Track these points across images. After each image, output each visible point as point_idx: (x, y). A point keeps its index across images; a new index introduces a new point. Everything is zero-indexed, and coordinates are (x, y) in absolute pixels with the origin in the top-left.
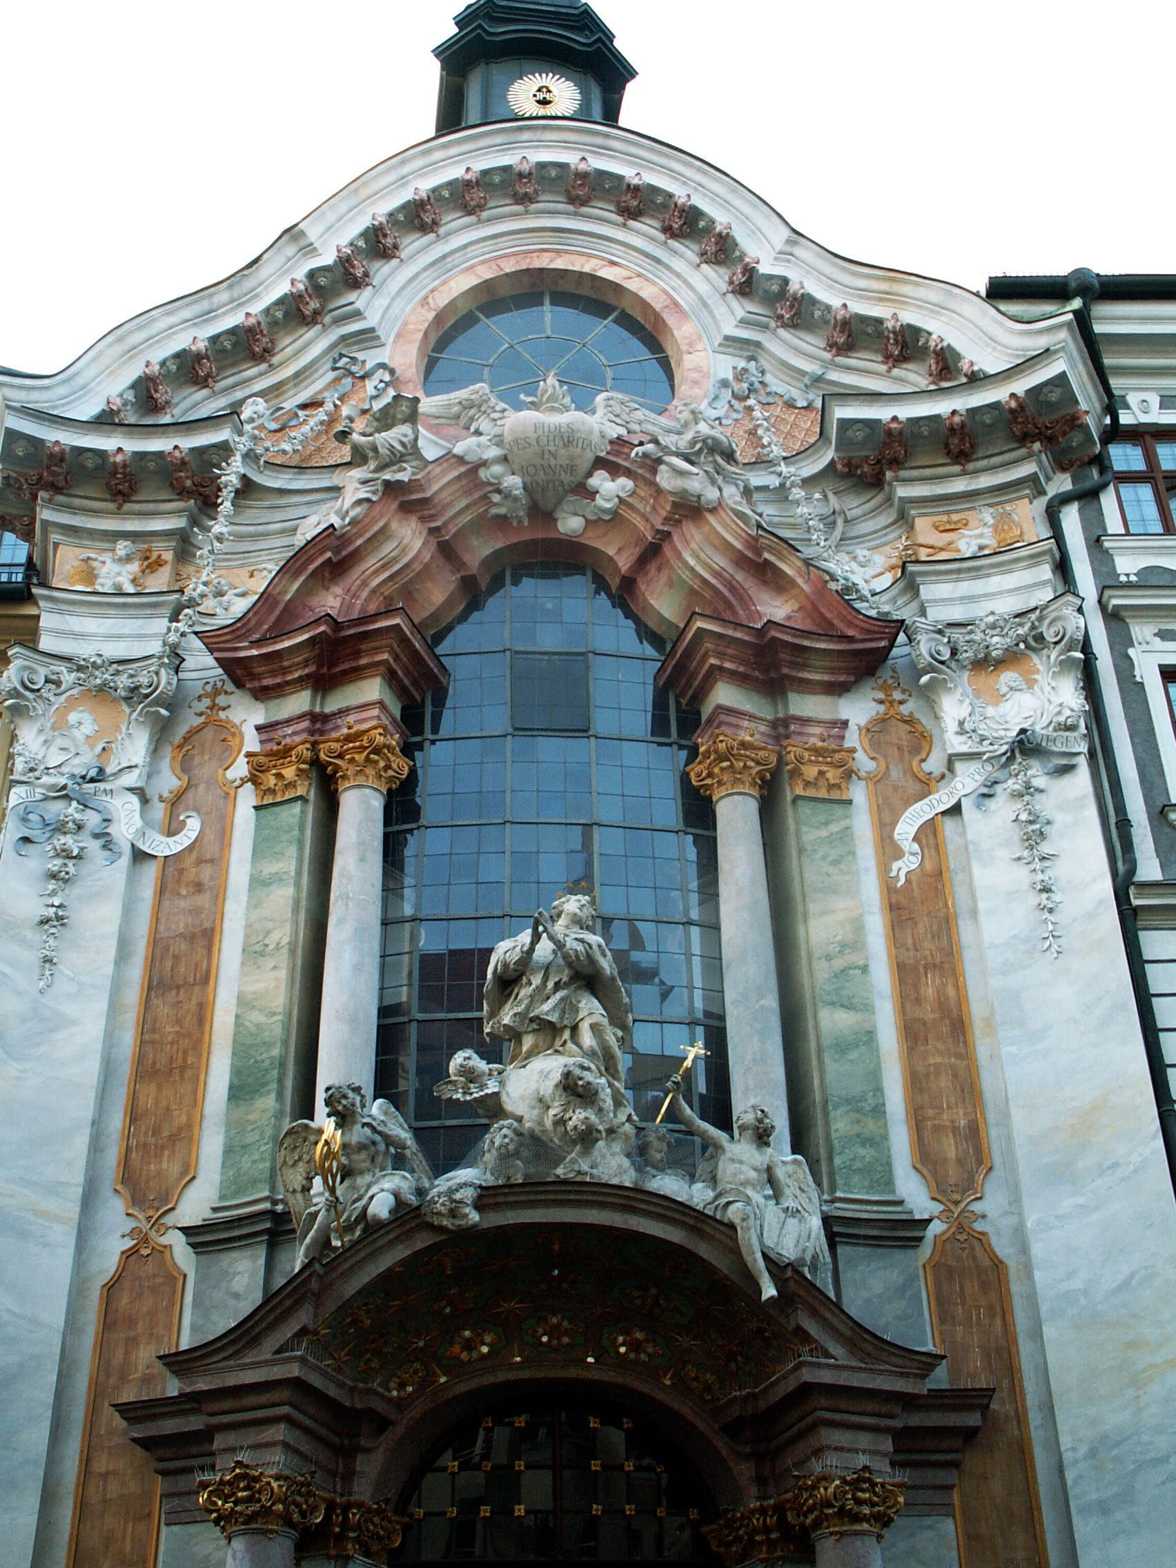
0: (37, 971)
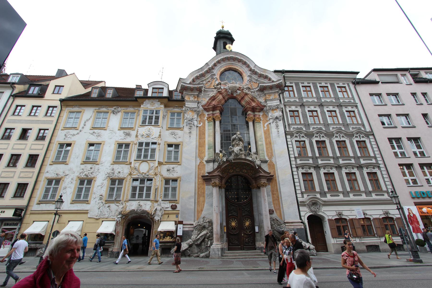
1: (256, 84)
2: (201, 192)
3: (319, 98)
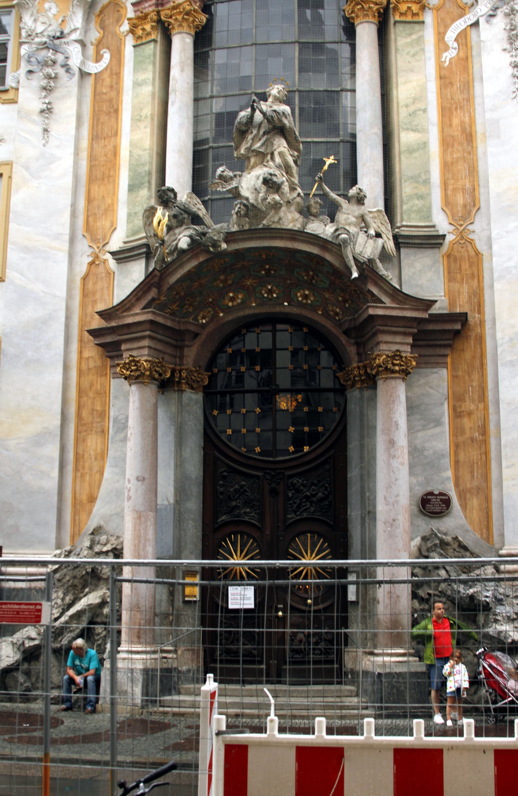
0: (41, 135)
2: (93, 410)
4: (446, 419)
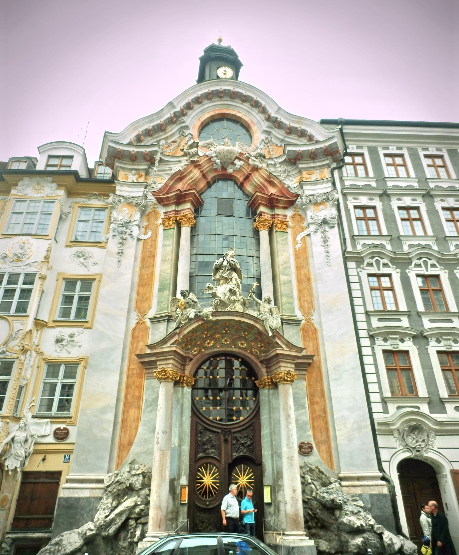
1: (281, 148)
3: (422, 179)
4: (307, 405)
